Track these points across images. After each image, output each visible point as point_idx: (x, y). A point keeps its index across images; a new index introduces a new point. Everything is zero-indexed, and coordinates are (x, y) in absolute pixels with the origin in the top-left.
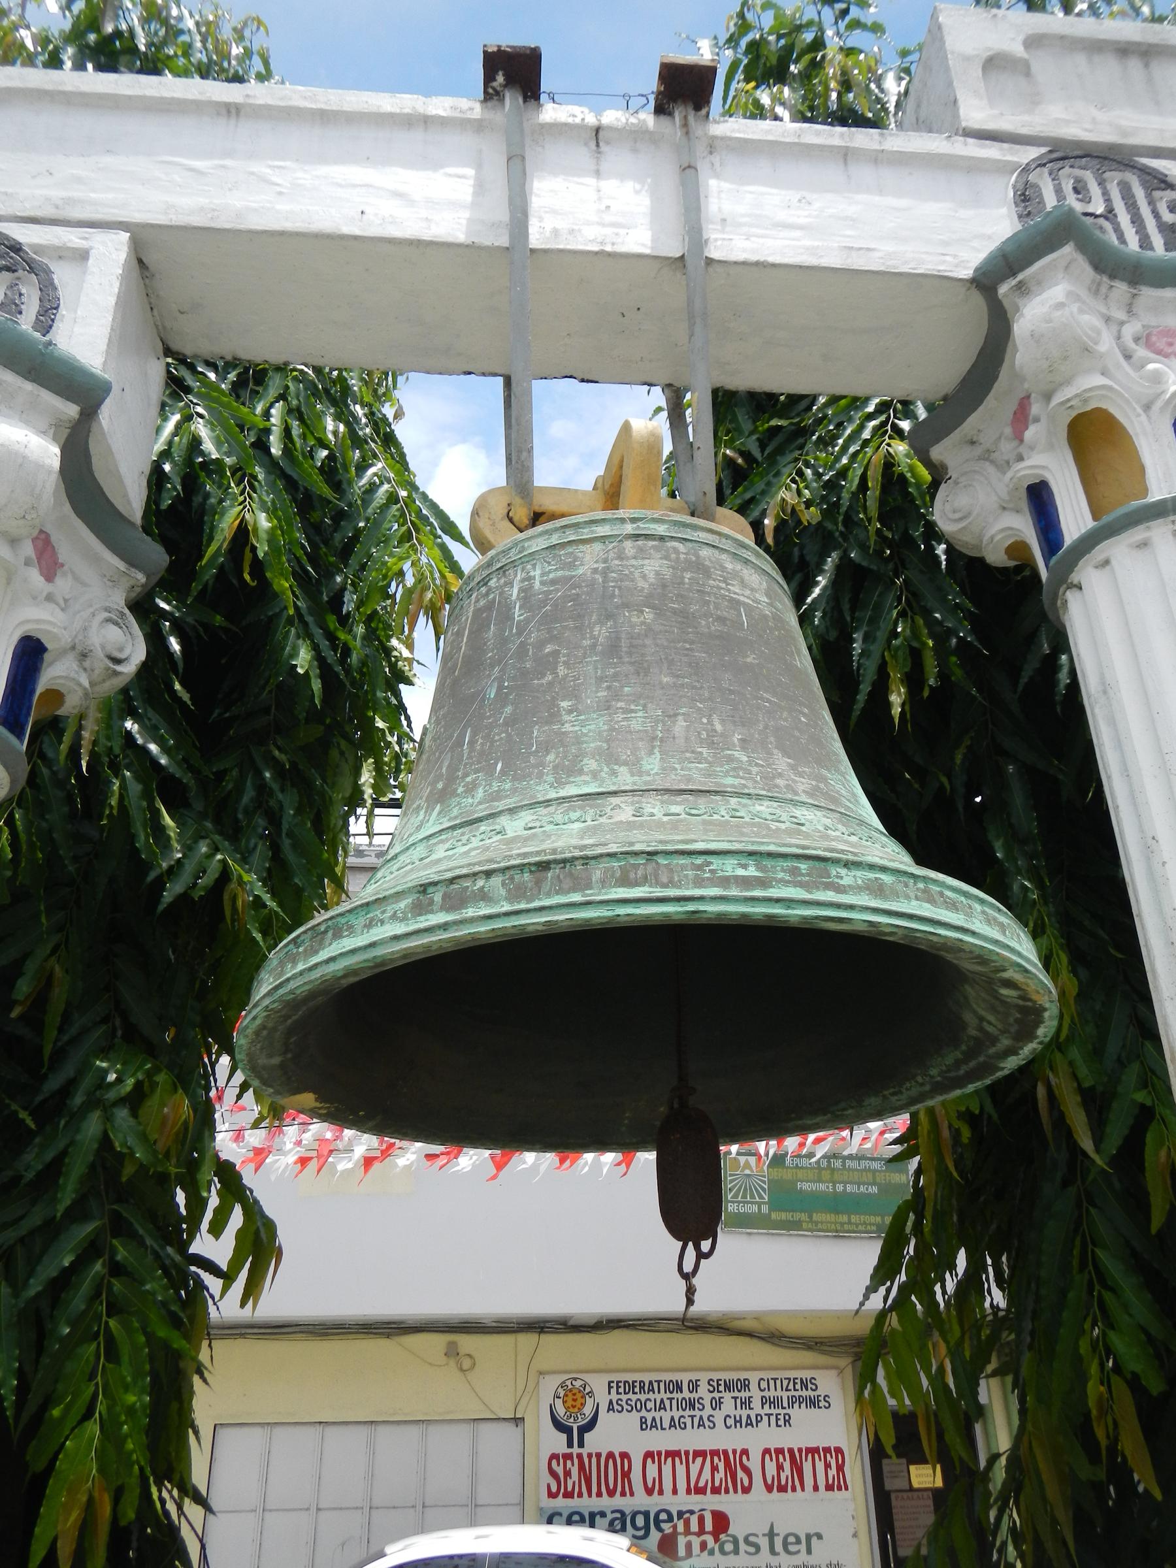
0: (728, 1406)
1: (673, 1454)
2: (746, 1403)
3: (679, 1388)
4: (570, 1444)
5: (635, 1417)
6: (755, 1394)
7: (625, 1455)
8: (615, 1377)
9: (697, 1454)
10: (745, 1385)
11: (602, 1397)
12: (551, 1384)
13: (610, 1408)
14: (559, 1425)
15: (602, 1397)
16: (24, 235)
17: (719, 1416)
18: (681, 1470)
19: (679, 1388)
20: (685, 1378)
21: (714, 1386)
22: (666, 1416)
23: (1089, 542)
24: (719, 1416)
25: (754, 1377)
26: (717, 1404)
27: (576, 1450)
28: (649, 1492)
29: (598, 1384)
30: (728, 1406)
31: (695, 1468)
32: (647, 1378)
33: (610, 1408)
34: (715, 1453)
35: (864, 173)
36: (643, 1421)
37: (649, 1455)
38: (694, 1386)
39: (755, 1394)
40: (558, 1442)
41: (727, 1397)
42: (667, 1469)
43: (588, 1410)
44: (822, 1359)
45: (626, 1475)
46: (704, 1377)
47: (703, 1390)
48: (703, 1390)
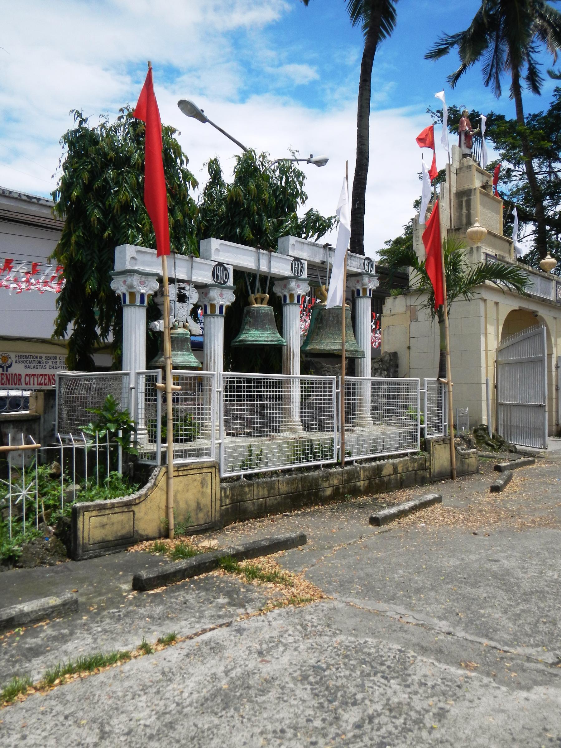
0: (50, 363)
1: (34, 375)
2: (56, 363)
3: (37, 358)
4: (3, 371)
5: (23, 365)
6: (58, 361)
7: (20, 375)
8: (18, 354)
9: (41, 375)
10: (56, 358)
11: (14, 359)
13: (16, 362)
15: (14, 359)
16: (226, 266)
17: (47, 366)
18: (36, 379)
19: (37, 358)
20: (38, 355)
21: (47, 358)
22: (32, 365)
23: (288, 304)
24: (47, 366)
25: (58, 356)
26: (47, 363)
27: (5, 373)
28: (26, 384)
29: (13, 355)
30: (50, 363)
31: (40, 379)
32: (27, 354)
33: (16, 362)
34: (46, 375)
35: (281, 260)
36: (25, 366)
37: (27, 375)
38: (41, 357)
39: (58, 361)
41: (50, 361)
42: (32, 379)
43: (9, 362)
45: (20, 380)
46: (44, 355)
47: (43, 359)
48: (43, 359)
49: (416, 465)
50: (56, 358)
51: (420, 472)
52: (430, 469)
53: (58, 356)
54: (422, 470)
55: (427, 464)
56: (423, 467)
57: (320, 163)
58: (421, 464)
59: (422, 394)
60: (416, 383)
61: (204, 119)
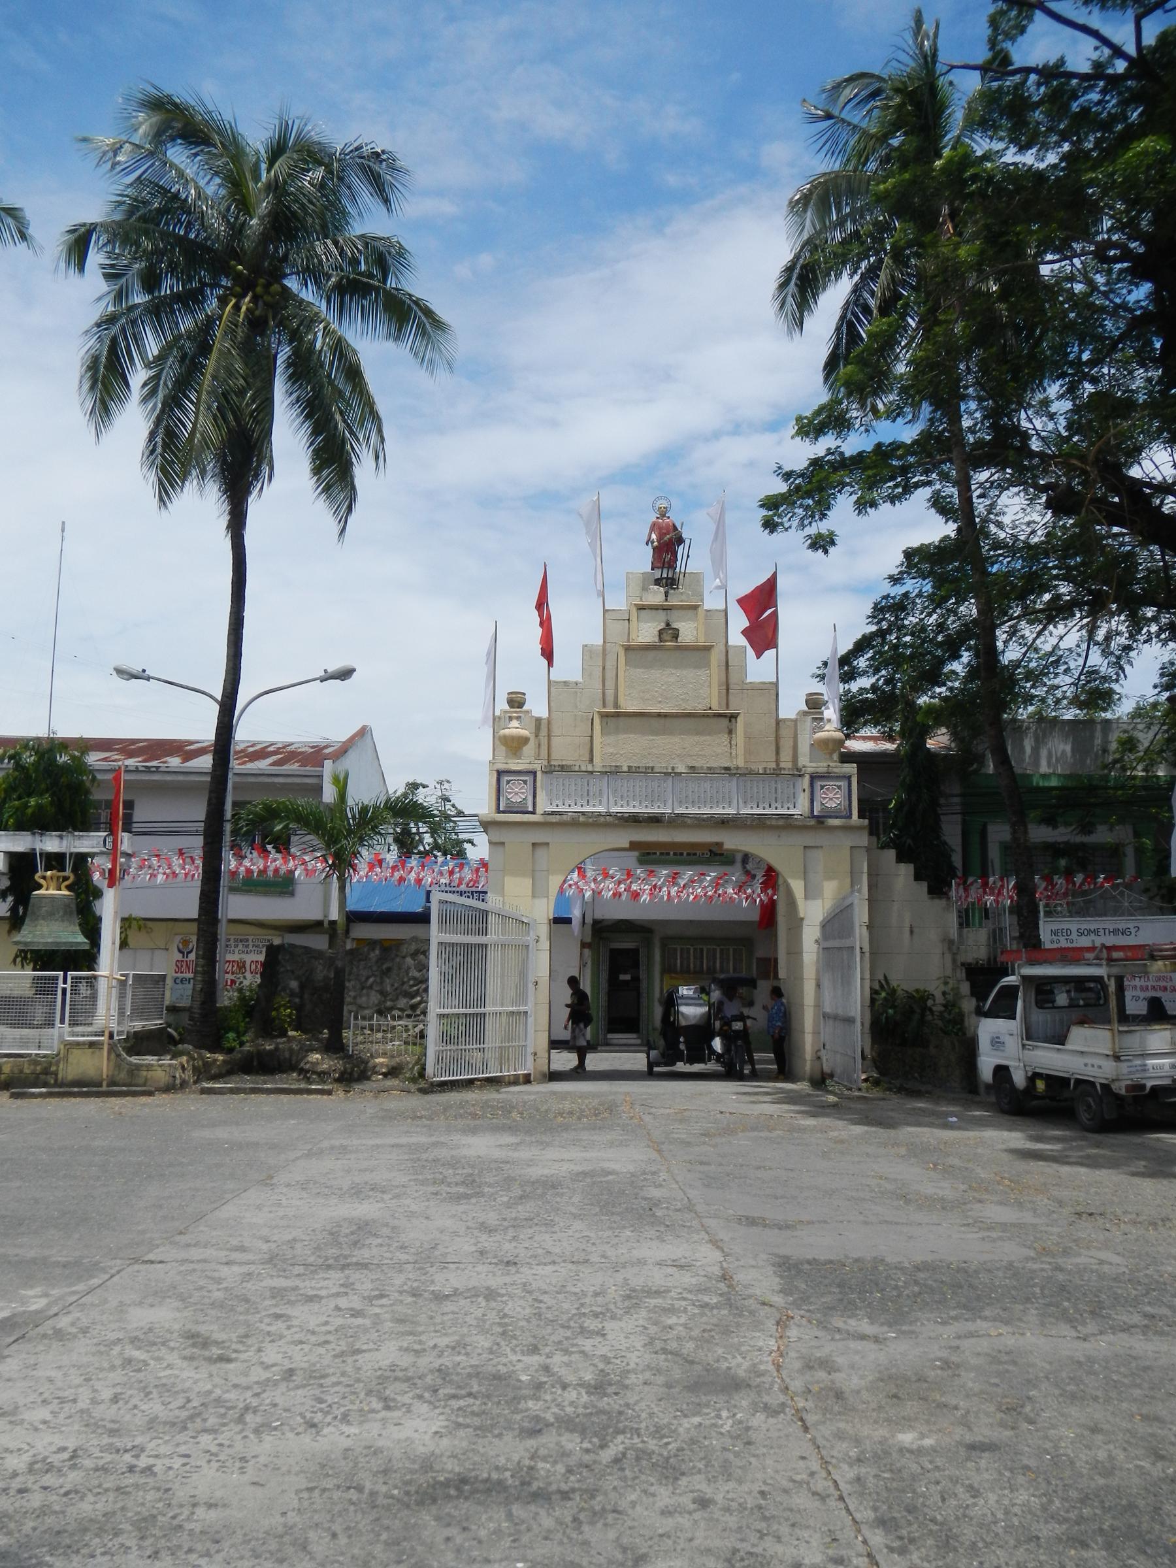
0: (240, 947)
2: (247, 946)
6: (251, 943)
12: (178, 938)
14: (180, 951)
21: (236, 940)
25: (250, 938)
26: (236, 946)
30: (240, 947)
39: (251, 943)
40: (180, 956)
44: (277, 933)
46: (232, 937)
47: (232, 942)
48: (232, 942)
49: (39, 1068)
50: (247, 940)
51: (42, 1077)
52: (56, 1075)
53: (250, 938)
54: (46, 1074)
55: (53, 1068)
56: (46, 1072)
57: (345, 674)
58: (46, 1068)
59: (64, 990)
60: (56, 978)
61: (148, 679)
